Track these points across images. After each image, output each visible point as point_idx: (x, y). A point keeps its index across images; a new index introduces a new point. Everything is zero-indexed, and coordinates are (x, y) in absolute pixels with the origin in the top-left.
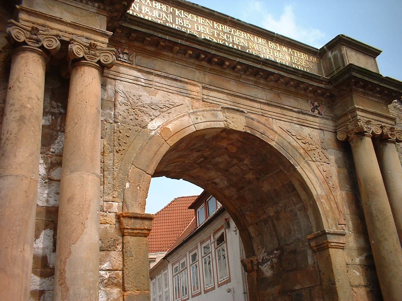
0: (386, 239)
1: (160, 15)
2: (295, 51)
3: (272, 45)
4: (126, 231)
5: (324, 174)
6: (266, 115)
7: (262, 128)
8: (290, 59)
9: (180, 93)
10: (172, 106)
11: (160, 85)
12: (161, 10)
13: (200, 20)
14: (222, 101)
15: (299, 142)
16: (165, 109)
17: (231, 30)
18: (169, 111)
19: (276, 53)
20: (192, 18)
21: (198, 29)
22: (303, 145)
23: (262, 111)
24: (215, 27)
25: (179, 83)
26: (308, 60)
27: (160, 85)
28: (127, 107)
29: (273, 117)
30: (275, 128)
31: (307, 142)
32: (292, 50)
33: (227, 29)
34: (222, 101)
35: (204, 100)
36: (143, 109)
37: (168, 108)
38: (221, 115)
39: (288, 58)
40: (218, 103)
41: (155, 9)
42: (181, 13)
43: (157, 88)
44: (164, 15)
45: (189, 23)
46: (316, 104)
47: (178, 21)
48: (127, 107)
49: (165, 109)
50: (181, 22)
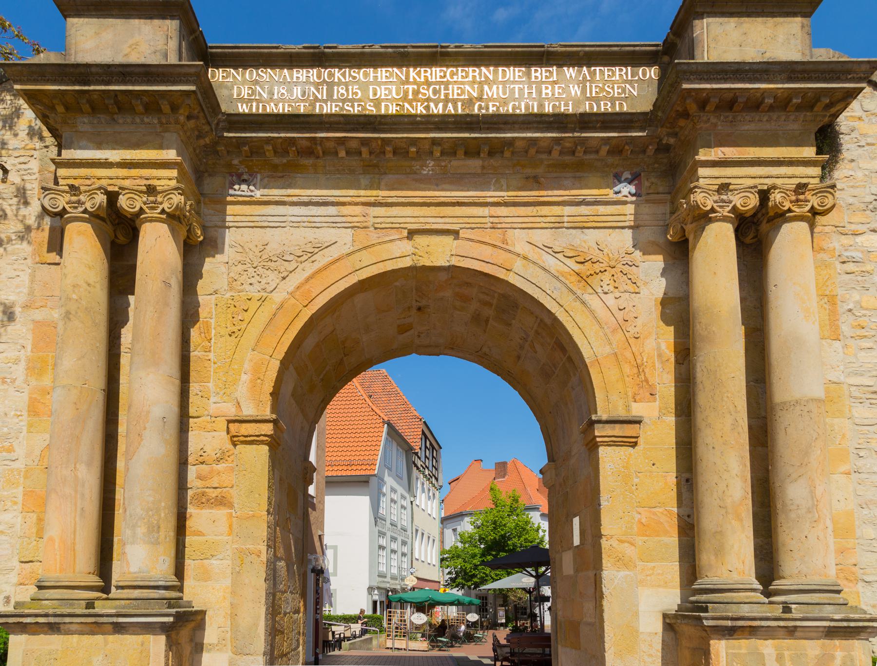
0: (709, 425)
1: (305, 92)
2: (598, 68)
3: (539, 73)
4: (235, 439)
5: (620, 315)
6: (499, 226)
8: (579, 93)
9: (334, 225)
10: (317, 250)
11: (299, 219)
12: (307, 82)
13: (382, 73)
14: (408, 220)
15: (568, 261)
16: (305, 257)
17: (445, 72)
18: (313, 259)
19: (547, 88)
20: (366, 75)
21: (375, 94)
22: (576, 267)
23: (492, 220)
24: (411, 80)
26: (629, 78)
27: (299, 219)
28: (245, 267)
29: (515, 226)
30: (521, 247)
31: (587, 259)
32: (589, 72)
33: (435, 73)
34: (408, 220)
35: (376, 226)
36: (269, 263)
37: (310, 255)
38: (406, 247)
39: (575, 90)
40: (402, 225)
41: (296, 84)
42: (344, 75)
43: (295, 224)
44: (313, 89)
45: (358, 89)
47: (338, 92)
48: (245, 267)
49: (305, 257)
50: (343, 91)
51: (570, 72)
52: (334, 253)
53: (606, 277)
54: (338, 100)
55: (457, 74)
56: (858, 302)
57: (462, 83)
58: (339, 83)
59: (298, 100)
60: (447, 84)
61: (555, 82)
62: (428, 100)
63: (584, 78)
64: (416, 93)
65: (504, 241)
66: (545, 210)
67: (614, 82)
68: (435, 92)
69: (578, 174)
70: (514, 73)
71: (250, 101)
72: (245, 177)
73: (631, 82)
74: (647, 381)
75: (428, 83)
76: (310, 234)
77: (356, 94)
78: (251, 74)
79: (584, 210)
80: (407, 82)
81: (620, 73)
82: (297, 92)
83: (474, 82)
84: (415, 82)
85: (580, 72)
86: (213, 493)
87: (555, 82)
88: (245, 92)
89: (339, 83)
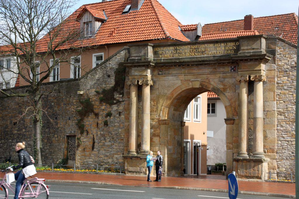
3: (216, 45)
7: (206, 84)
9: (177, 80)
13: (186, 47)
20: (183, 47)
25: (177, 76)
38: (191, 84)
42: (179, 48)
44: (173, 51)
46: (233, 67)
51: (222, 44)
52: (177, 85)
53: (228, 89)
54: (178, 53)
55: (200, 46)
56: (280, 93)
57: (201, 48)
58: (178, 50)
59: (171, 54)
60: (198, 49)
61: (220, 47)
62: (195, 52)
63: (225, 45)
64: (193, 51)
65: (209, 82)
66: (217, 75)
67: (231, 46)
68: (196, 50)
69: (224, 67)
70: (212, 45)
71: (162, 54)
72: (161, 71)
73: (234, 46)
74: (236, 111)
75: (195, 49)
76: (173, 82)
77: (181, 52)
78: (162, 48)
79: (224, 75)
80: (191, 49)
81: (232, 44)
82: (170, 52)
83: (204, 48)
84: (192, 49)
85: (224, 44)
86: (156, 134)
87: (220, 47)
88: (161, 53)
89: (178, 50)
